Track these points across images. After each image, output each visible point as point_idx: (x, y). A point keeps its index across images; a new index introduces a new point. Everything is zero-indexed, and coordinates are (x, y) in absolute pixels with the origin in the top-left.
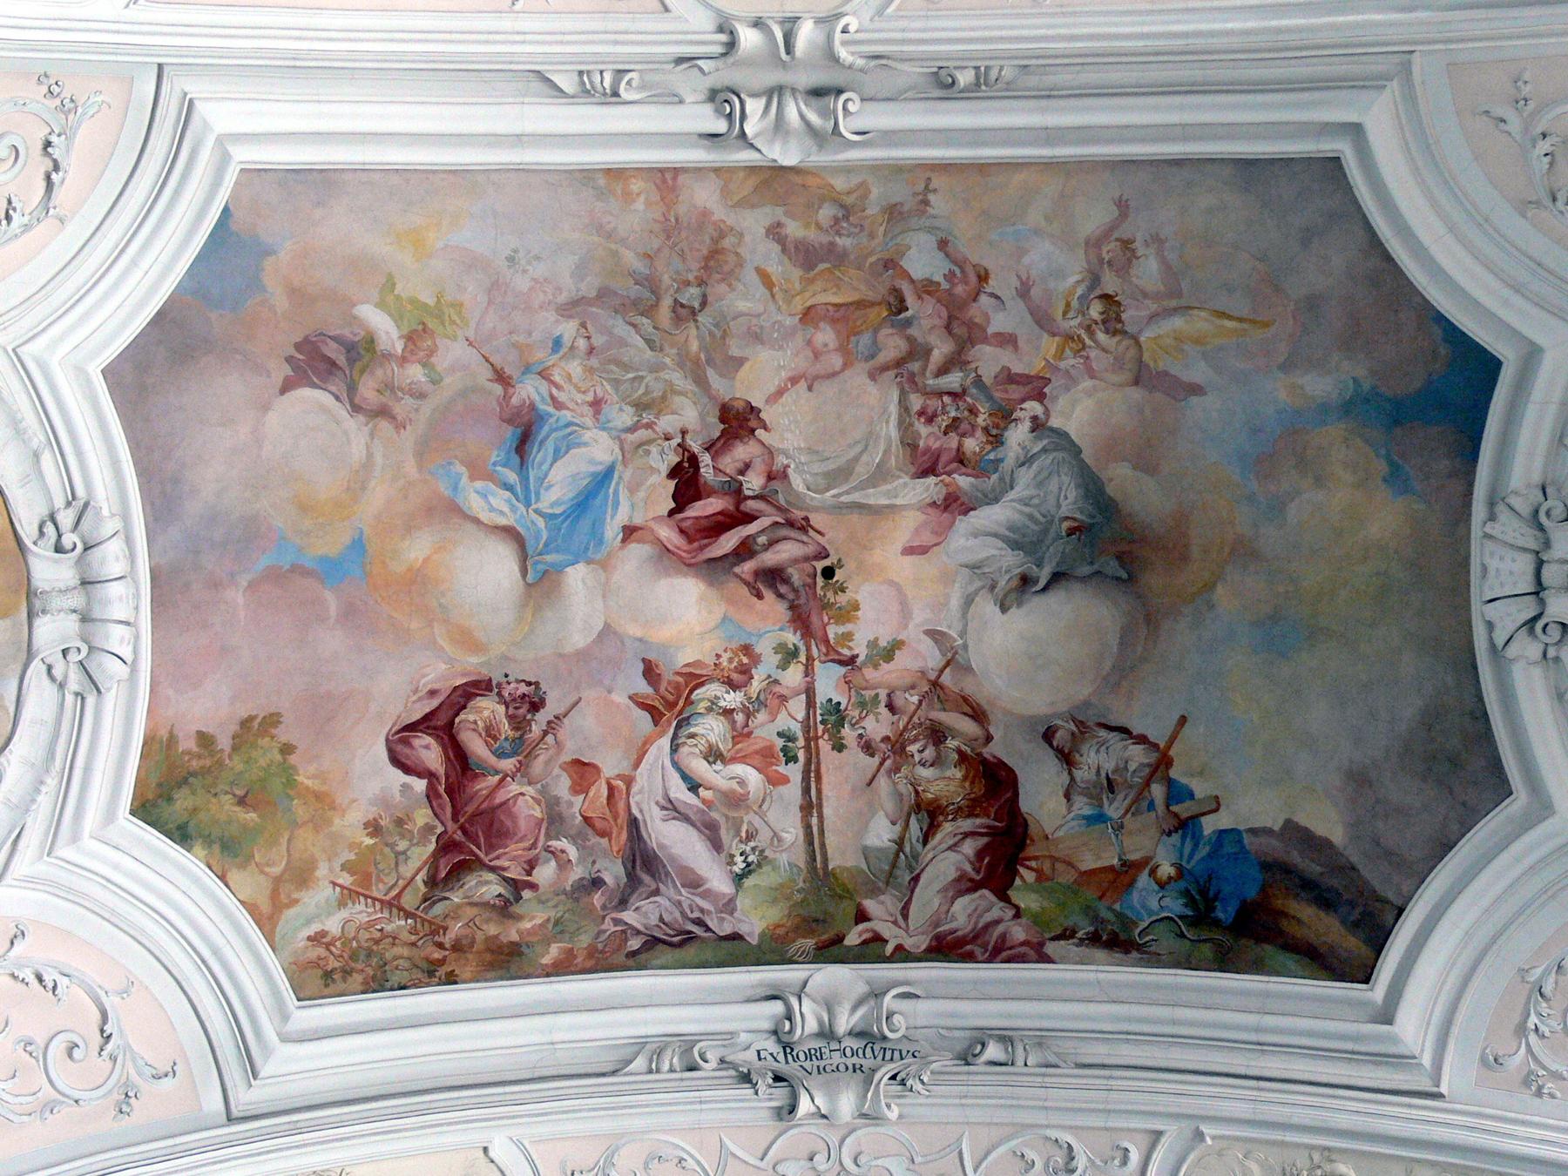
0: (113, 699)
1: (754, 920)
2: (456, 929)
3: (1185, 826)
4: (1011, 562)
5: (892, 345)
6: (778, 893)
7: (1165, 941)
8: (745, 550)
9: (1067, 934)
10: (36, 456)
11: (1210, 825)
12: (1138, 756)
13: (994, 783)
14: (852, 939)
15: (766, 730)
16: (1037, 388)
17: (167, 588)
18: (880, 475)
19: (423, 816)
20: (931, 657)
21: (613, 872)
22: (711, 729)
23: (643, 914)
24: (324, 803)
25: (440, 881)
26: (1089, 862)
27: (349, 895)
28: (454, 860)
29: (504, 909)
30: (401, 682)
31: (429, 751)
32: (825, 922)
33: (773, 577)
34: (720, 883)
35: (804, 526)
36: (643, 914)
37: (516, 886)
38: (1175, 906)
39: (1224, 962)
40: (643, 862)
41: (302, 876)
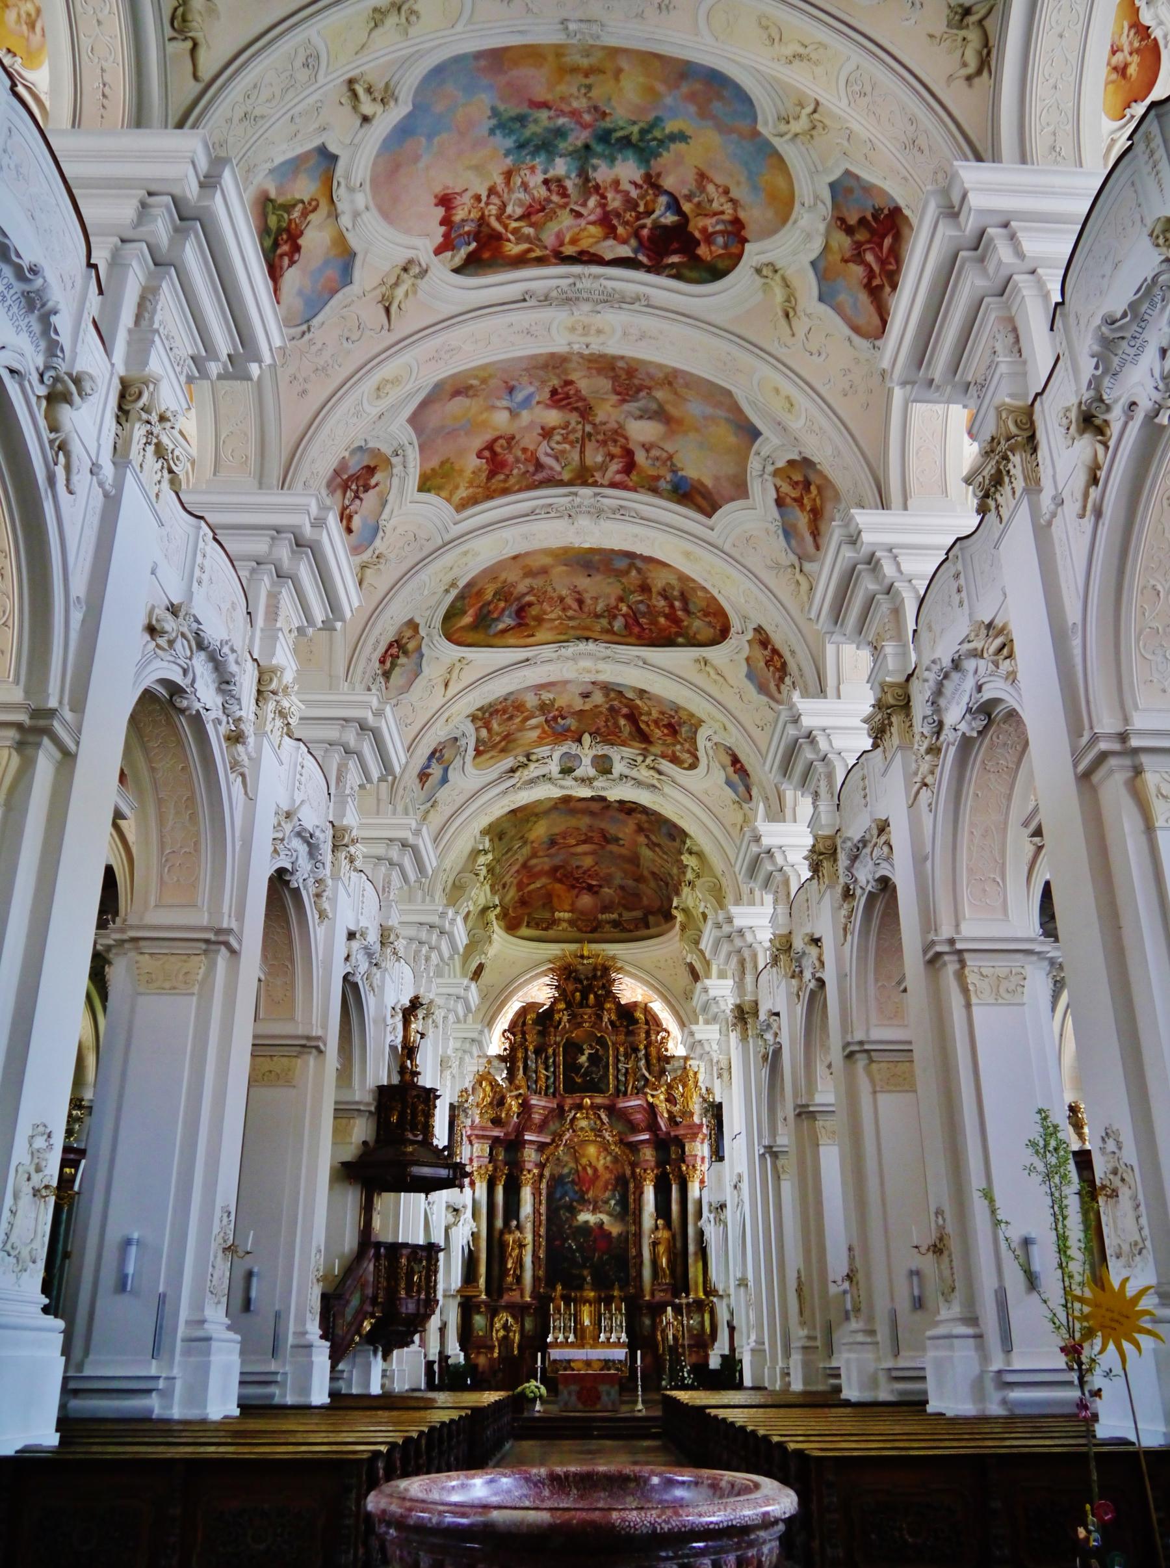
0: (411, 477)
1: (566, 476)
2: (493, 487)
3: (674, 472)
4: (638, 413)
5: (612, 374)
6: (572, 471)
7: (665, 494)
8: (569, 404)
9: (643, 487)
11: (680, 473)
12: (665, 455)
13: (629, 454)
14: (591, 481)
15: (572, 437)
16: (650, 388)
17: (422, 448)
18: (606, 393)
19: (485, 467)
20: (615, 426)
21: (532, 469)
22: (558, 438)
23: (539, 477)
24: (461, 471)
25: (489, 478)
26: (650, 473)
27: (467, 488)
28: (492, 474)
29: (505, 481)
30: (478, 442)
31: (487, 454)
32: (583, 477)
33: (576, 409)
34: (558, 468)
35: (585, 400)
36: (539, 477)
37: (508, 476)
38: (669, 487)
39: (679, 502)
40: (539, 466)
41: (457, 487)
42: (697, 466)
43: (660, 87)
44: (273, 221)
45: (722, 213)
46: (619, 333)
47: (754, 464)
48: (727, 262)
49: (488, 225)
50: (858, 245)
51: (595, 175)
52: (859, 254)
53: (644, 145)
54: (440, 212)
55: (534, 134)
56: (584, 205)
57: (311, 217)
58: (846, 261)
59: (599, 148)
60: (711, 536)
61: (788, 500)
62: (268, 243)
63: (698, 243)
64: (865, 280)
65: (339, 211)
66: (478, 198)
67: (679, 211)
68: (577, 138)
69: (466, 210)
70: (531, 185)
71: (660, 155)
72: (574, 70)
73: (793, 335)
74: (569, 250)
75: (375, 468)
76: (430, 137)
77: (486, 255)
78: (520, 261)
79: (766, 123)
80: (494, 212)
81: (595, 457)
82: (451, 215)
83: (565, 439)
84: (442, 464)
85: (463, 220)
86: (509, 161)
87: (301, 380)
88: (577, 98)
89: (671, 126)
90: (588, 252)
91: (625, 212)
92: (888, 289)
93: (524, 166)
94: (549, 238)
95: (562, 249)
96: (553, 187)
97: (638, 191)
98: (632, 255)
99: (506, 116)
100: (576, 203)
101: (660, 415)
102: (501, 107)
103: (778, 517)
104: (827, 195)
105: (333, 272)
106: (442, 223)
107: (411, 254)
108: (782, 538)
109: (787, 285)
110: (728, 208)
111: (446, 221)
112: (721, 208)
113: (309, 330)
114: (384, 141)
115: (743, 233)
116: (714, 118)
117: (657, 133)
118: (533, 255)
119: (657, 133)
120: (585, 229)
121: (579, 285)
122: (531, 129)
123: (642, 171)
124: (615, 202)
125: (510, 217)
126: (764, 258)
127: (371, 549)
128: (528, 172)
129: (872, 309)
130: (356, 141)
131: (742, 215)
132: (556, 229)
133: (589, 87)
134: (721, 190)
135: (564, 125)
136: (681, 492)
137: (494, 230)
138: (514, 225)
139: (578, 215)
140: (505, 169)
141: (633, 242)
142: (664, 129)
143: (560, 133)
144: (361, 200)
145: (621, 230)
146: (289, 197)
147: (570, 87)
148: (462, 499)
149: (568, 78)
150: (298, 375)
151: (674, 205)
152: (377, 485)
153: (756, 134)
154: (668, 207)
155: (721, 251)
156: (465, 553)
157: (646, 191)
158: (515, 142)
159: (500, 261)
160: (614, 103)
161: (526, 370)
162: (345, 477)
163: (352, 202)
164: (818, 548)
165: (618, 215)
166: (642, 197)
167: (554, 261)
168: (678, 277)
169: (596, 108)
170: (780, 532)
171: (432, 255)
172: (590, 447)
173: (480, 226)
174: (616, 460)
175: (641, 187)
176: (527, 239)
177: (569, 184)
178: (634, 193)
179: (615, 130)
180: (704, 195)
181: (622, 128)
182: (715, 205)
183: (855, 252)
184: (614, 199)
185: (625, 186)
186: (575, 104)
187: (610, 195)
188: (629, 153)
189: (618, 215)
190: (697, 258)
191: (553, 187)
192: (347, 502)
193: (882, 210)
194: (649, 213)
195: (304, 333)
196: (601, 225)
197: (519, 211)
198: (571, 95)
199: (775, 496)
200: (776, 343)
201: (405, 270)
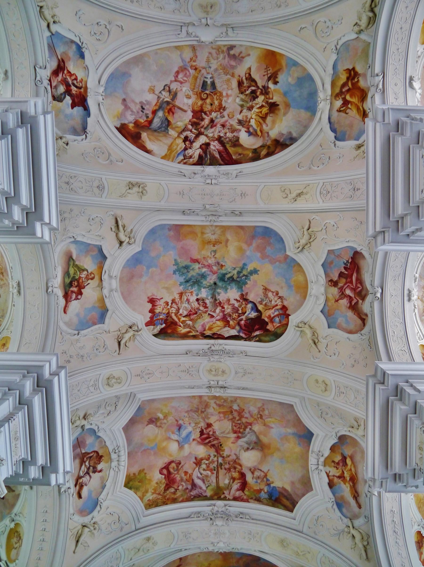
2: (168, 496)
3: (269, 485)
4: (246, 446)
5: (231, 417)
6: (213, 490)
7: (265, 501)
8: (210, 442)
9: (252, 498)
10: (113, 442)
11: (272, 485)
12: (262, 474)
13: (243, 476)
14: (222, 497)
15: (212, 466)
16: (251, 424)
17: (130, 455)
18: (228, 433)
19: (164, 481)
20: (234, 457)
21: (190, 487)
22: (204, 466)
23: (193, 493)
24: (150, 480)
26: (255, 488)
27: (153, 493)
28: (168, 487)
29: (174, 493)
30: (161, 463)
31: (165, 471)
32: (218, 494)
33: (213, 446)
35: (218, 439)
37: (176, 490)
38: (266, 496)
39: (273, 506)
40: (194, 485)
41: (147, 491)
42: (282, 478)
43: (244, 246)
44: (72, 271)
45: (277, 305)
46: (233, 372)
47: (312, 460)
48: (282, 329)
49: (171, 317)
50: (342, 290)
51: (219, 297)
52: (343, 293)
53: (239, 280)
54: (150, 306)
55: (192, 276)
56: (214, 312)
57: (89, 281)
58: (337, 301)
59: (220, 284)
60: (295, 524)
61: (336, 480)
62: (68, 281)
63: (267, 324)
64: (348, 305)
65: (103, 286)
66: (167, 303)
67: (258, 311)
68: (211, 279)
69: (161, 308)
70: (191, 301)
71: (246, 283)
72: (209, 242)
73: (320, 351)
74: (208, 333)
75: (101, 457)
76: (148, 267)
77: (169, 331)
78: (185, 336)
79: (290, 249)
80: (174, 311)
81: (225, 481)
82: (154, 309)
83: (208, 468)
84: (140, 472)
85: (160, 313)
86: (181, 288)
87: (68, 355)
88: (210, 258)
89: (250, 267)
90: (217, 334)
91: (233, 314)
92: (360, 301)
93: (188, 291)
94: (199, 328)
95: (205, 332)
96: (201, 302)
97: (238, 303)
98: (238, 334)
99: (181, 265)
100: (211, 311)
101: (259, 445)
102: (179, 260)
103: (331, 495)
104: (322, 272)
105: (95, 314)
106: (150, 312)
107: (134, 321)
108: (337, 510)
109: (310, 327)
110: (279, 302)
111: (152, 311)
112: (276, 303)
113: (78, 334)
114: (128, 260)
115: (287, 313)
116: (268, 256)
117: (245, 272)
118: (191, 334)
119: (245, 272)
120: (215, 323)
121: (213, 348)
122: (192, 273)
123: (239, 293)
124: (228, 309)
125: (181, 315)
126: (298, 320)
127: (90, 516)
128: (190, 294)
129: (355, 318)
130: (116, 255)
131: (285, 303)
132: (202, 323)
133: (215, 252)
134: (274, 294)
135: (205, 272)
136: (273, 498)
137: (173, 319)
138: (183, 319)
139: (212, 316)
140: (180, 292)
141: (238, 328)
142: (247, 269)
143: (203, 276)
144: (115, 284)
145: (231, 323)
146: (81, 265)
147: (206, 252)
148: (149, 500)
149: (206, 246)
150: (67, 352)
151: (255, 308)
152: (100, 471)
153: (287, 257)
154: (252, 309)
155: (279, 325)
156: (148, 539)
157: (242, 303)
158: (184, 279)
159: (176, 335)
160: (226, 260)
161: (187, 412)
162: (83, 451)
163: (110, 284)
164: (360, 507)
165: (230, 316)
166: (240, 306)
167: (201, 337)
168: (260, 341)
169: (218, 263)
170: (335, 506)
171: (144, 326)
172: (222, 472)
173: (167, 317)
174: (236, 481)
175: (240, 301)
176: (189, 326)
177: (207, 302)
178: (237, 305)
179: (227, 274)
180: (267, 299)
181: (230, 273)
182: (273, 303)
183: (340, 293)
184: (228, 308)
185: (233, 302)
186: (210, 262)
187: (226, 306)
188: (233, 285)
189: (230, 316)
190: (268, 330)
191: (201, 302)
192: (82, 474)
193: (348, 261)
194: (244, 313)
195: (75, 335)
196: (222, 321)
197: (185, 313)
198: (208, 256)
199: (327, 480)
200: (312, 359)
201: (130, 327)
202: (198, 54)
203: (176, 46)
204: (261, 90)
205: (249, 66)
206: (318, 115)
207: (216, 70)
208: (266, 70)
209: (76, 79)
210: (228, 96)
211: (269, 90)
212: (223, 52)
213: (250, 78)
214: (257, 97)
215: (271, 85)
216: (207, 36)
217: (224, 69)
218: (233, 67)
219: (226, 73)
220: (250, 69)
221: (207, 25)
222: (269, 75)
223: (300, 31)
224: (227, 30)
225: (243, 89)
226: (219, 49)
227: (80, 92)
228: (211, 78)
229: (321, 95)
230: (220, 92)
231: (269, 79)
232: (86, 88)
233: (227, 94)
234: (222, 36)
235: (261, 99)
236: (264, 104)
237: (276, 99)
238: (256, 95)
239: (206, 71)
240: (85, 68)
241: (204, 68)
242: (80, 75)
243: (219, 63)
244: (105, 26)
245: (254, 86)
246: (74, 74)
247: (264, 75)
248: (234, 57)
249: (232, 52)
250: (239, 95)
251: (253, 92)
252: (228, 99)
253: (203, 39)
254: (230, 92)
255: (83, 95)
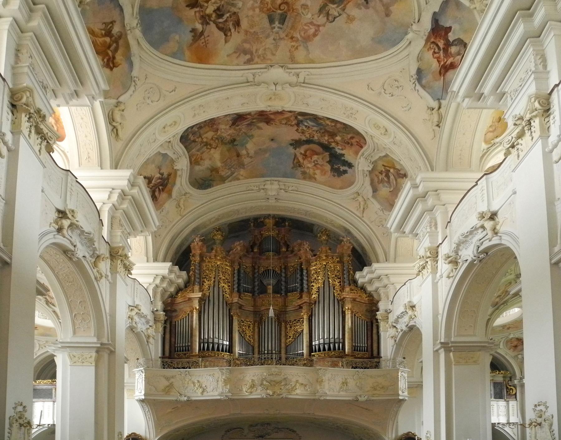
202: (288, 54)
203: (313, 63)
204: (210, 20)
205: (227, 44)
206: (136, 9)
207: (268, 37)
208: (207, 42)
209: (434, 53)
210: (253, 9)
211: (200, 21)
212: (259, 57)
213: (225, 30)
214: (214, 11)
215: (199, 27)
216: (277, 73)
217: (257, 38)
218: (245, 41)
219: (256, 33)
220: (226, 42)
221: (275, 85)
222: (203, 37)
223: (176, 88)
224: (254, 79)
225: (234, 18)
226: (264, 59)
227: (436, 38)
228: (274, 28)
229: (138, 33)
230: (263, 12)
231: (202, 33)
232: (427, 41)
233: (254, 11)
234: (260, 74)
235: (210, 9)
236: (206, 5)
237: (191, 13)
238: (216, 13)
239: (279, 36)
240: (421, 60)
241: (281, 39)
242: (429, 55)
243: (263, 44)
244: (386, 92)
245: (220, 23)
246: (435, 58)
247: (208, 36)
248: (245, 52)
249: (248, 57)
250: (238, 10)
251: (220, 16)
252: (253, 5)
253: (281, 70)
254: (251, 13)
255: (433, 35)
